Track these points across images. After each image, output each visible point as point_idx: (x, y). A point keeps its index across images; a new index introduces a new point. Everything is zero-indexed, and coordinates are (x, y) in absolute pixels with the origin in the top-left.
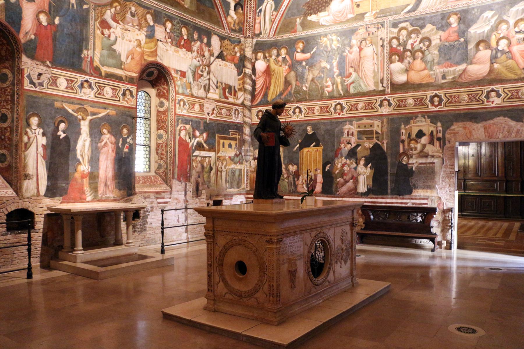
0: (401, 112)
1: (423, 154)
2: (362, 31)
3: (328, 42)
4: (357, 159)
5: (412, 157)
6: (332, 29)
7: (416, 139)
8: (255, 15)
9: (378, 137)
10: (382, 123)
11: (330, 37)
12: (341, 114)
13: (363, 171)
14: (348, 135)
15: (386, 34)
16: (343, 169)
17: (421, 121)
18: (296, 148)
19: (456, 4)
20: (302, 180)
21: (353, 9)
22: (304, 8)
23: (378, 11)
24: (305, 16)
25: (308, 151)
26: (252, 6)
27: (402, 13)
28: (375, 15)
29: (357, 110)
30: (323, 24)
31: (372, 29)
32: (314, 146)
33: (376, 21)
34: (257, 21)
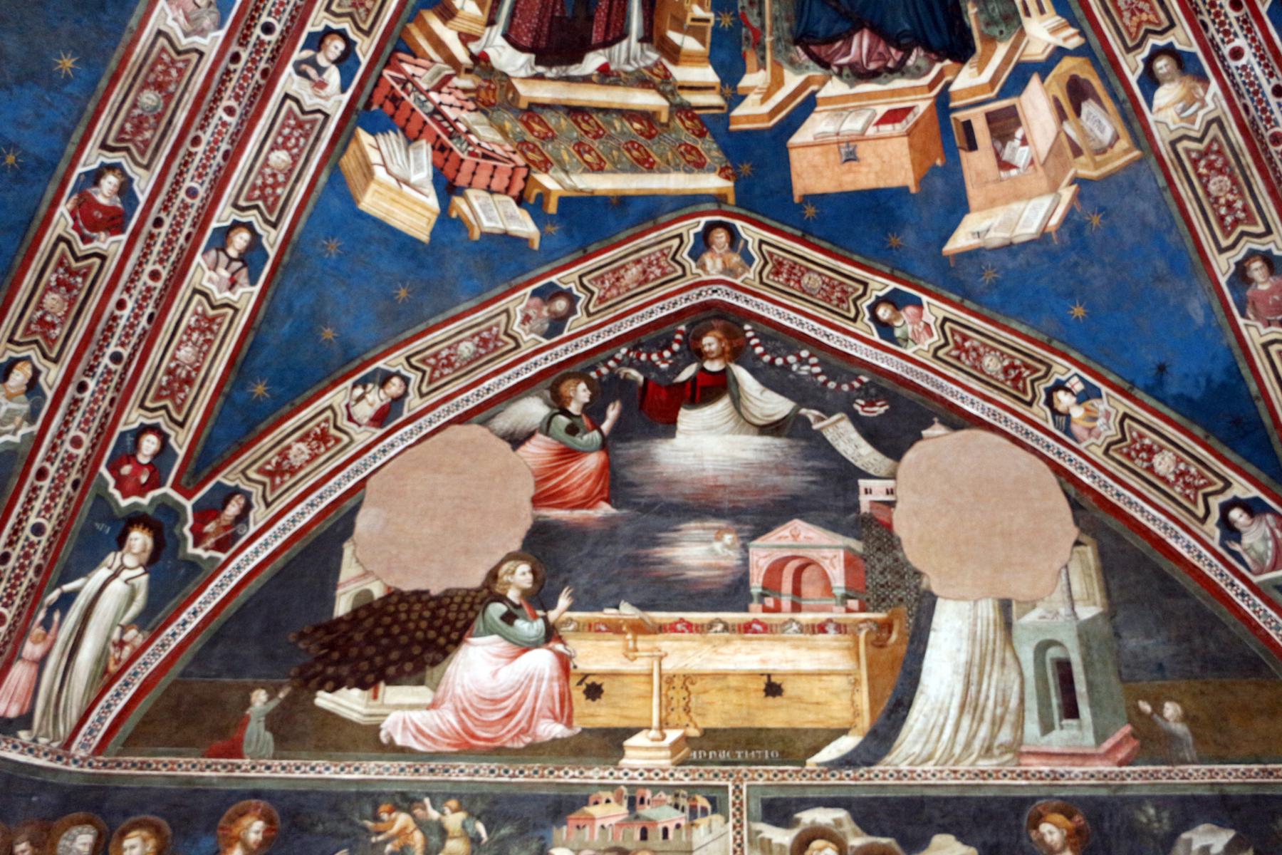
2: (608, 813)
3: (418, 837)
6: (445, 777)
8: (31, 615)
11: (434, 814)
15: (731, 846)
19: (1061, 770)
21: (565, 698)
22: (301, 645)
23: (693, 732)
24: (306, 681)
26: (37, 559)
27: (813, 761)
28: (675, 747)
30: (399, 741)
31: (664, 815)
33: (682, 777)
34: (32, 649)
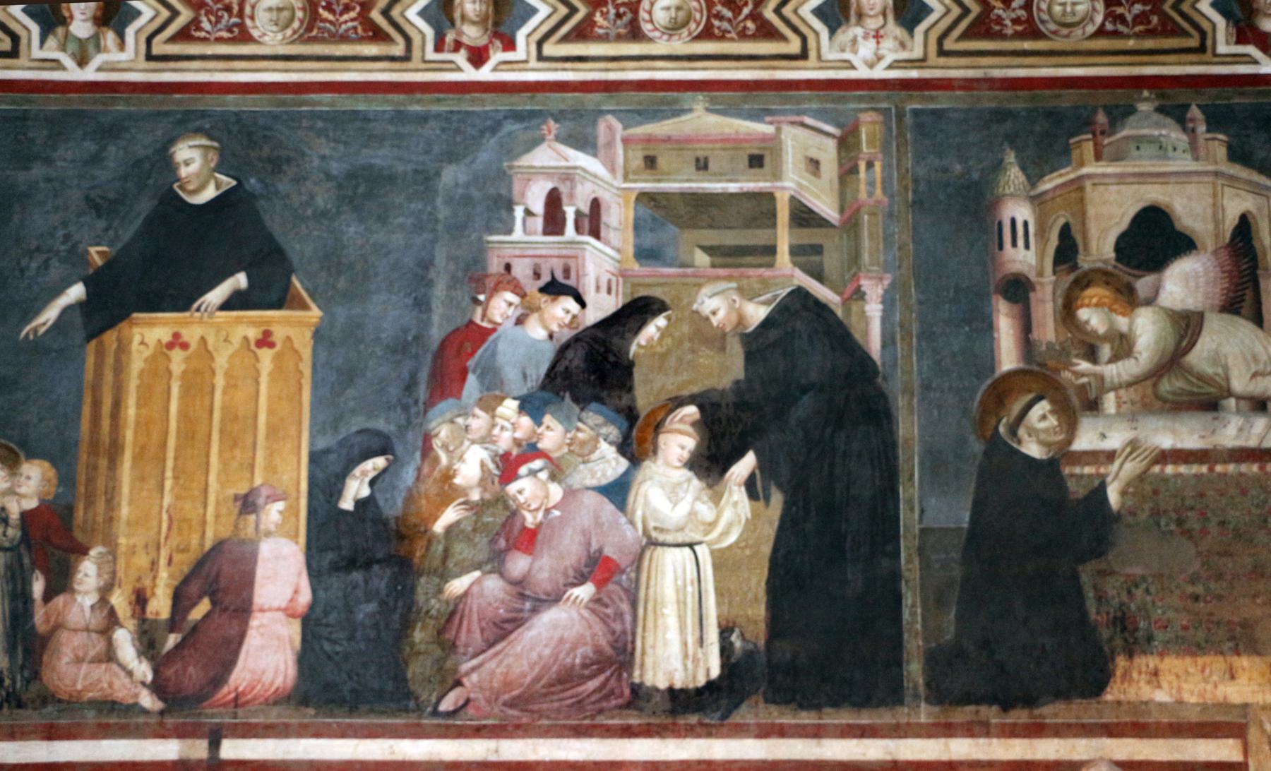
0: (997, 73)
1: (1179, 384)
4: (630, 415)
5: (1093, 406)
7: (1124, 273)
9: (817, 250)
10: (847, 143)
12: (497, 56)
13: (682, 509)
14: (554, 222)
16: (501, 500)
17: (1161, 147)
18: (51, 314)
20: (105, 592)
25: (177, 342)
29: (635, 33)
32: (235, 302)
